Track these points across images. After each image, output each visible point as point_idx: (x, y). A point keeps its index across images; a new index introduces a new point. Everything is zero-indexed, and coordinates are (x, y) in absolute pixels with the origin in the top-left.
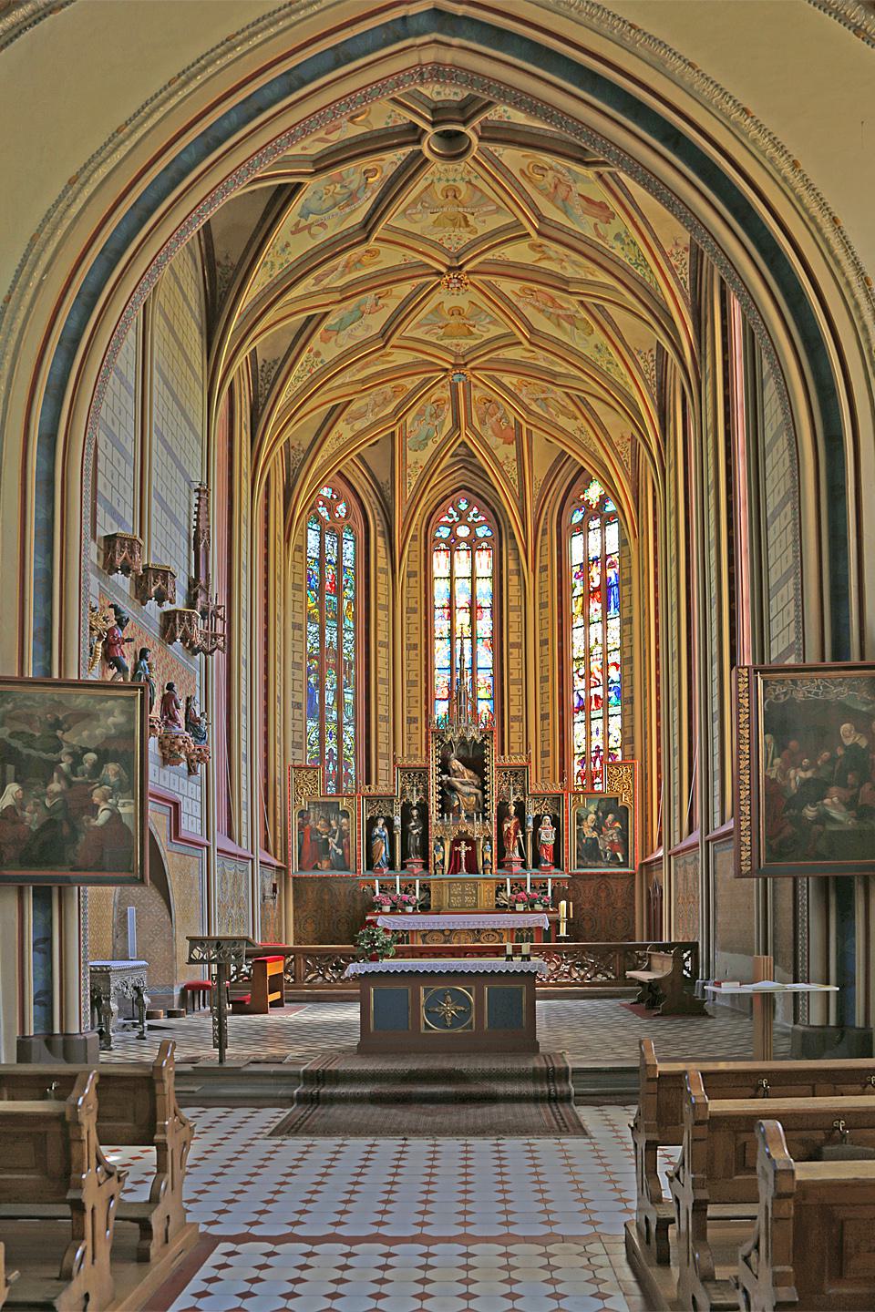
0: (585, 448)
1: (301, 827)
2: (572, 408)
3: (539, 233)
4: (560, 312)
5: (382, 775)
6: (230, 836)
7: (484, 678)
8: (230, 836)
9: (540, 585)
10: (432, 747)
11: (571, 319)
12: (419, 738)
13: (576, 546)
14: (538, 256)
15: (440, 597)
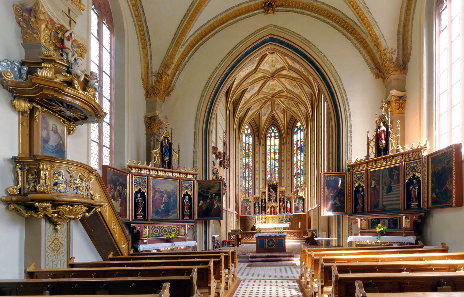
0: (297, 115)
1: (242, 205)
2: (295, 105)
3: (289, 69)
4: (293, 85)
5: (257, 192)
6: (229, 207)
7: (277, 169)
8: (229, 207)
9: (287, 147)
10: (266, 186)
11: (295, 86)
12: (264, 184)
13: (295, 136)
14: (288, 72)
15: (268, 151)
